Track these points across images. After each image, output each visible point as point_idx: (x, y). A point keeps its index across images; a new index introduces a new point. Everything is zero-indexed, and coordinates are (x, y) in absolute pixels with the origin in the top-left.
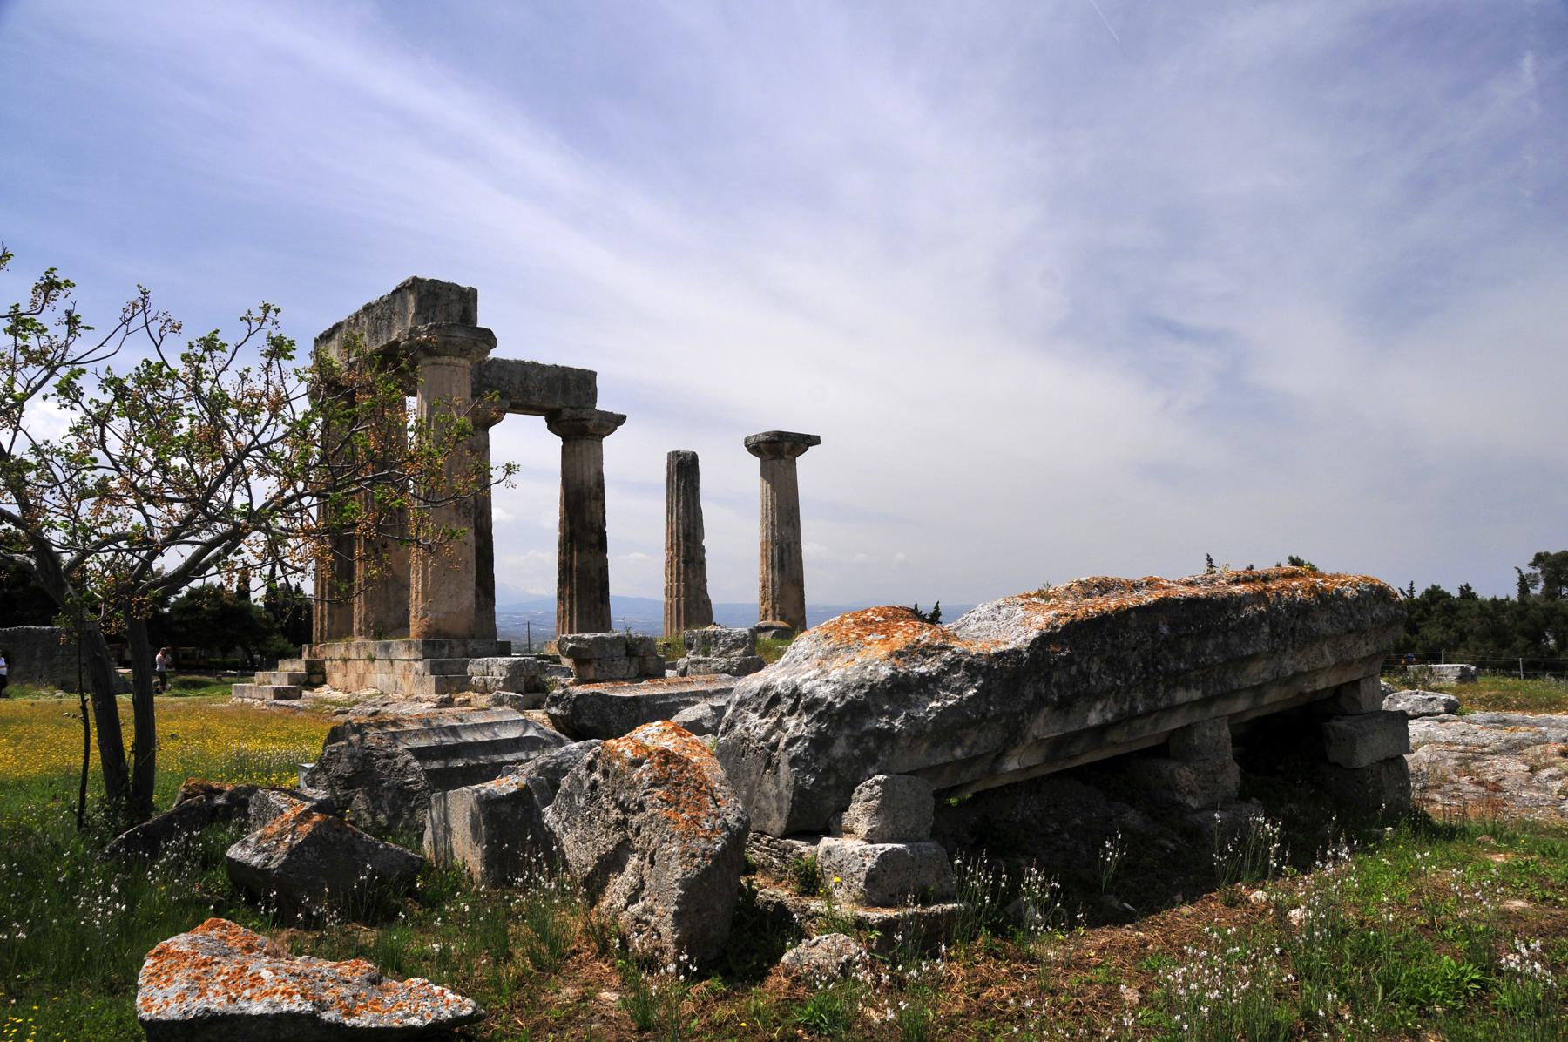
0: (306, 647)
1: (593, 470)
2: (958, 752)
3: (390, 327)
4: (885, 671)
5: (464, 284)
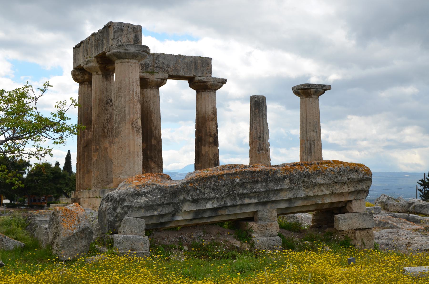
0: (73, 192)
1: (211, 107)
2: (156, 213)
3: (103, 44)
4: (132, 190)
5: (135, 23)
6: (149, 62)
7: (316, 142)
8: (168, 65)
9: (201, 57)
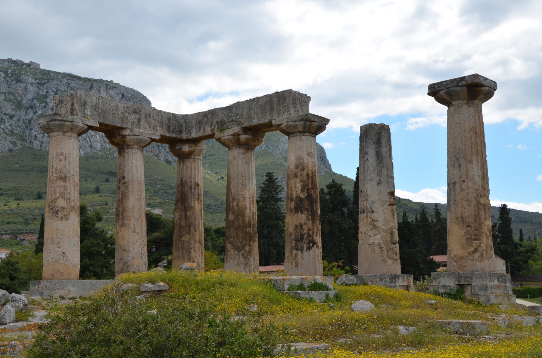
6: (224, 118)
7: (457, 185)
8: (242, 115)
9: (277, 93)
